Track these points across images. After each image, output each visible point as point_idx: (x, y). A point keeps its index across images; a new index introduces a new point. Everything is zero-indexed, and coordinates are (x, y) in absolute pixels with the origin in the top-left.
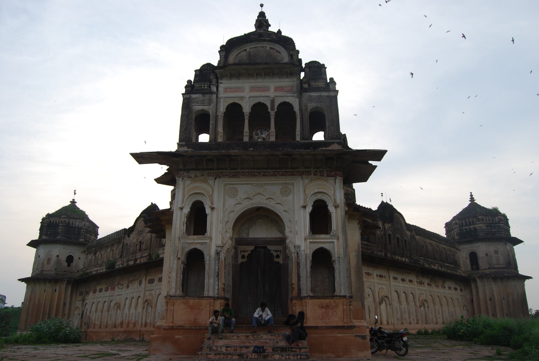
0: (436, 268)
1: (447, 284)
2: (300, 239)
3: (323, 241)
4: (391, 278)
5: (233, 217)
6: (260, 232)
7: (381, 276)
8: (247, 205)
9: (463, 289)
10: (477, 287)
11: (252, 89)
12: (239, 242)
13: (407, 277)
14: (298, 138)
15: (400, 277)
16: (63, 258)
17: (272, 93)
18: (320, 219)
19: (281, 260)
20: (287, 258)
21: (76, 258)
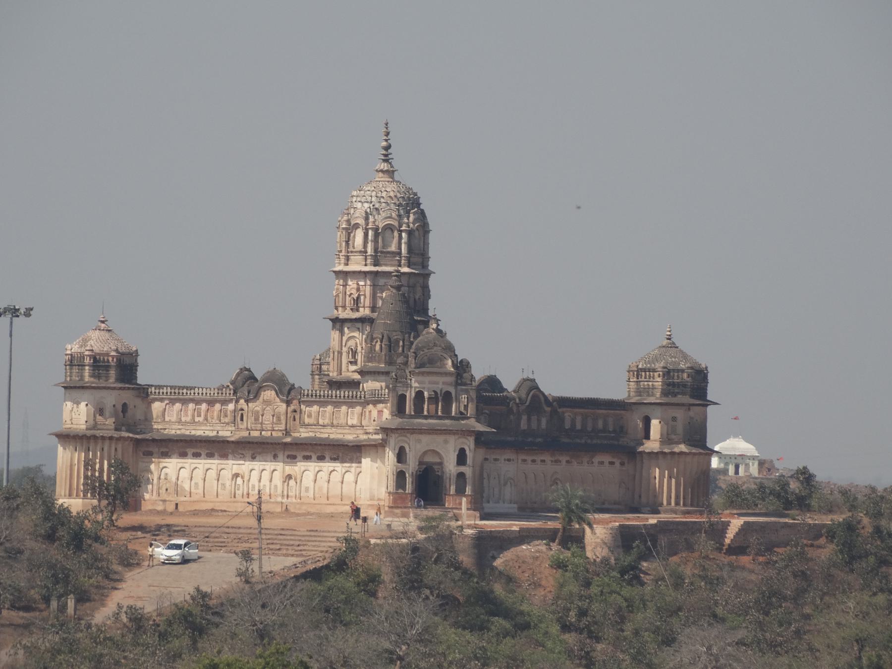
0: (583, 441)
1: (597, 459)
2: (451, 467)
3: (462, 469)
4: (520, 461)
5: (420, 454)
6: (429, 459)
7: (509, 460)
8: (427, 449)
9: (626, 461)
10: (642, 462)
11: (430, 383)
12: (421, 463)
13: (538, 458)
14: (453, 414)
15: (529, 458)
16: (120, 408)
17: (440, 386)
18: (461, 458)
19: (439, 474)
20: (443, 472)
21: (131, 406)
